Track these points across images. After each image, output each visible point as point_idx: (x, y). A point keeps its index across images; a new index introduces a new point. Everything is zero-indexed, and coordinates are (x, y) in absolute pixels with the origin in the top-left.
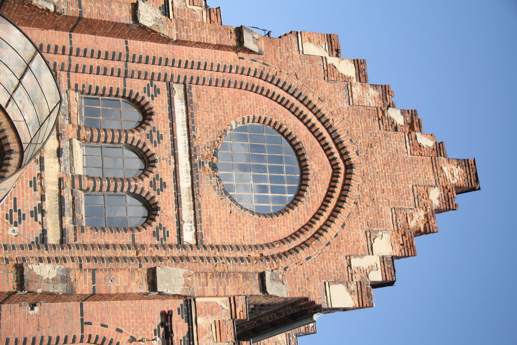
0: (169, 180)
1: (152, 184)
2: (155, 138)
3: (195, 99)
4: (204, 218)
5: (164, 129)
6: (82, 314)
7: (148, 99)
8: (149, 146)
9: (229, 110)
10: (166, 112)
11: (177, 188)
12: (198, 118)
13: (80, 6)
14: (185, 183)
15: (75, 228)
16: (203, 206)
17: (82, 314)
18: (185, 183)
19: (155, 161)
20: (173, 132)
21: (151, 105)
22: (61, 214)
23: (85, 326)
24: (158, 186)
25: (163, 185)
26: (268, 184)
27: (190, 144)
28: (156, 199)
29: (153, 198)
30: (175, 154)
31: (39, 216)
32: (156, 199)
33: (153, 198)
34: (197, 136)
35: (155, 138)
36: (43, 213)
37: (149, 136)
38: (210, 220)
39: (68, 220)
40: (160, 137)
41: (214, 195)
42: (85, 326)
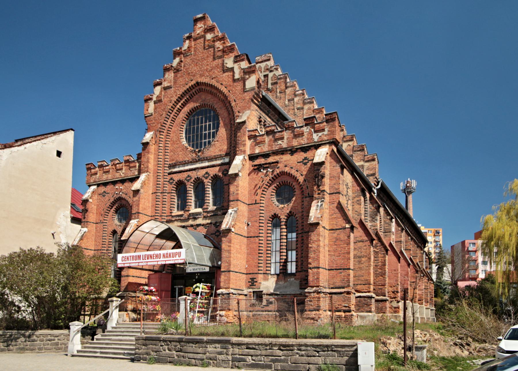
0: (204, 171)
1: (206, 178)
2: (189, 178)
3: (174, 162)
4: (220, 153)
5: (185, 175)
6: (252, 204)
7: (174, 183)
8: (192, 181)
9: (178, 146)
10: (179, 175)
11: (208, 167)
12: (181, 160)
13: (135, 214)
14: (207, 164)
15: (222, 210)
16: (215, 154)
17: (252, 204)
18: (207, 164)
19: (198, 178)
20: (187, 171)
21: (176, 181)
22: (217, 215)
23: (257, 202)
24: (207, 175)
25: (207, 173)
26: (207, 124)
27: (191, 162)
28: (212, 176)
29: (212, 177)
30: (194, 169)
31: (218, 224)
32: (212, 176)
33: (212, 177)
34: (188, 159)
35: (189, 178)
36: (216, 223)
37: (188, 181)
38: (220, 150)
39: (219, 213)
40: (189, 176)
41: (211, 149)
42: (257, 202)
